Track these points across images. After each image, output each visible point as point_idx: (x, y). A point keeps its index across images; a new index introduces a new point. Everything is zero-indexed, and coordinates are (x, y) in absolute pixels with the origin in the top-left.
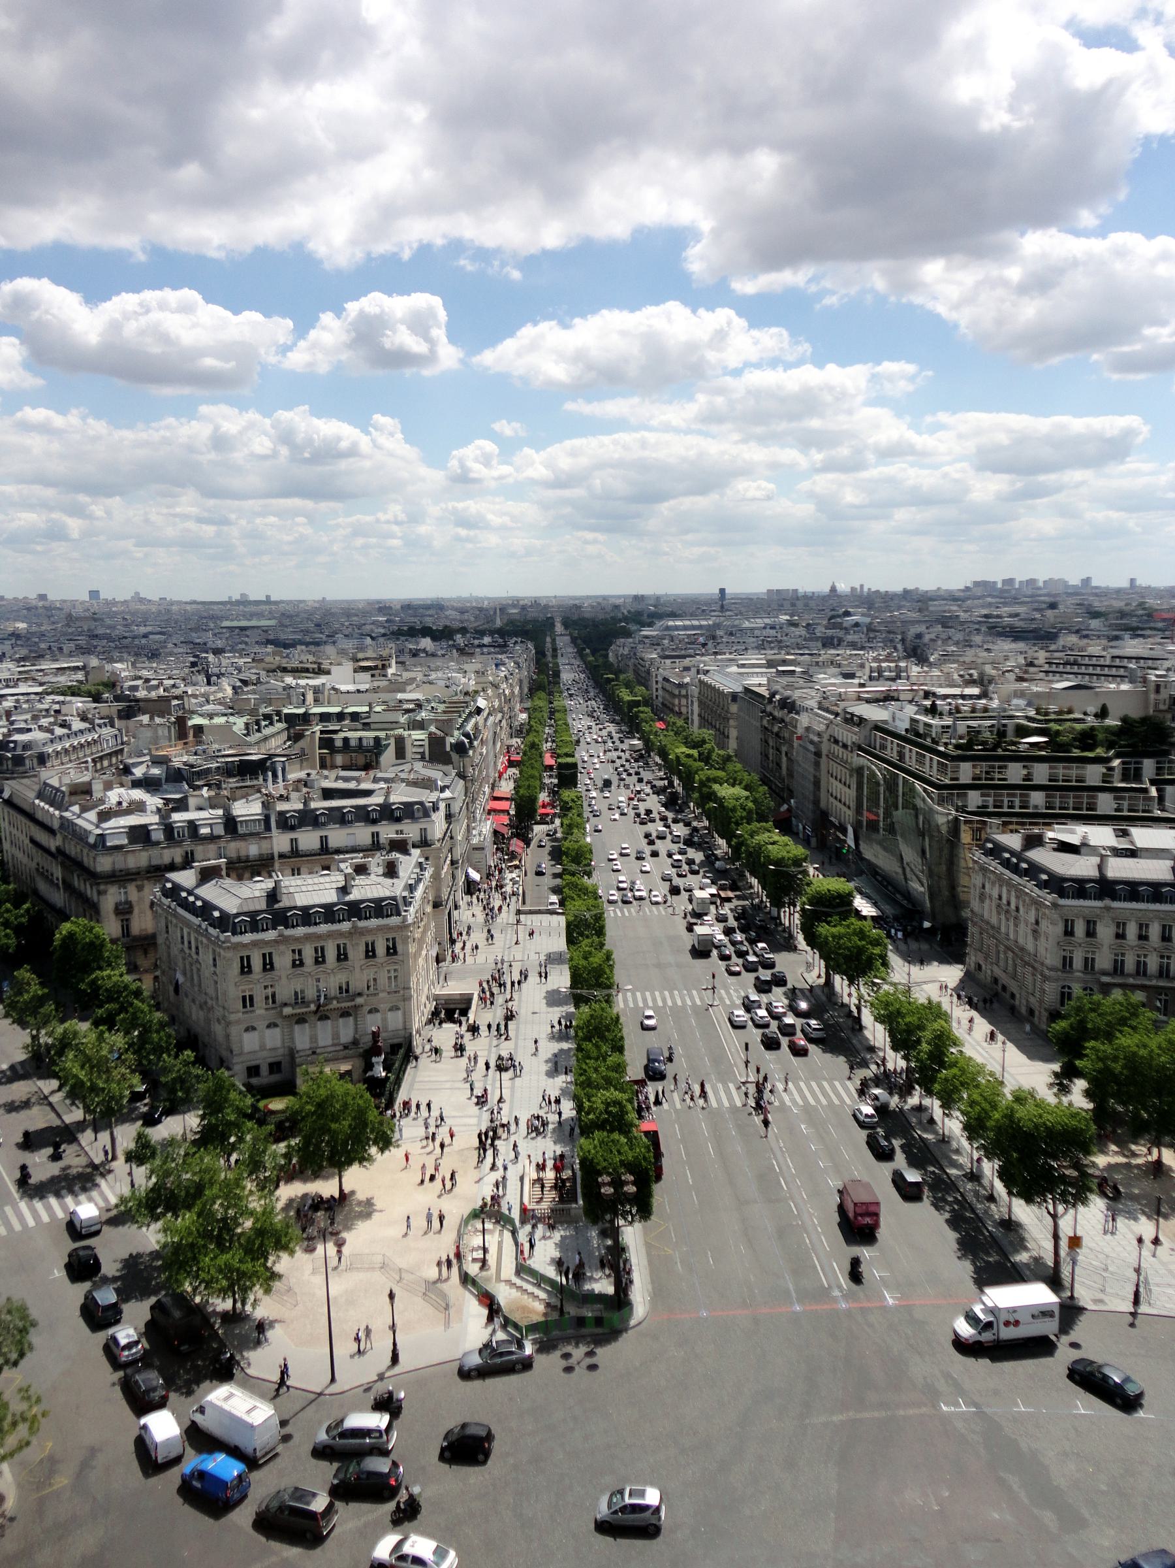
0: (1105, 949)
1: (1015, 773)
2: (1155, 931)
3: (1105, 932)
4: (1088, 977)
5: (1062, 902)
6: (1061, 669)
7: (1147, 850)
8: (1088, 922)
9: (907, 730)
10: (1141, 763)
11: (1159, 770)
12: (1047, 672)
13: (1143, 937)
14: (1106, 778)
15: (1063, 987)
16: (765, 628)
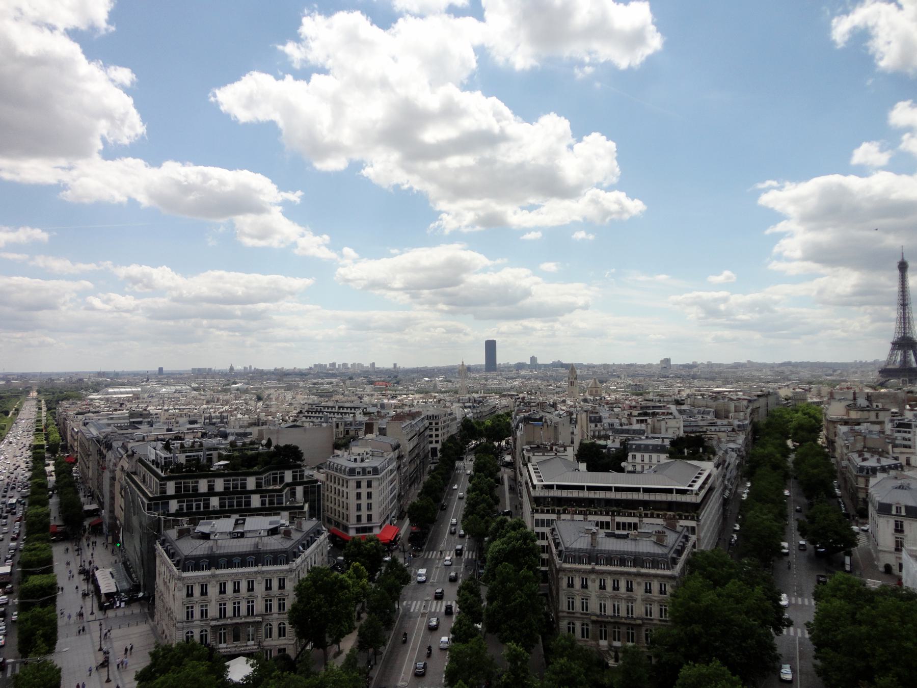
0: (214, 602)
1: (203, 485)
2: (244, 586)
3: (213, 591)
4: (203, 623)
5: (185, 574)
6: (314, 414)
7: (250, 531)
8: (202, 586)
9: (153, 461)
10: (284, 473)
11: (294, 477)
12: (306, 417)
13: (236, 590)
14: (258, 485)
15: (188, 633)
16: (175, 392)
